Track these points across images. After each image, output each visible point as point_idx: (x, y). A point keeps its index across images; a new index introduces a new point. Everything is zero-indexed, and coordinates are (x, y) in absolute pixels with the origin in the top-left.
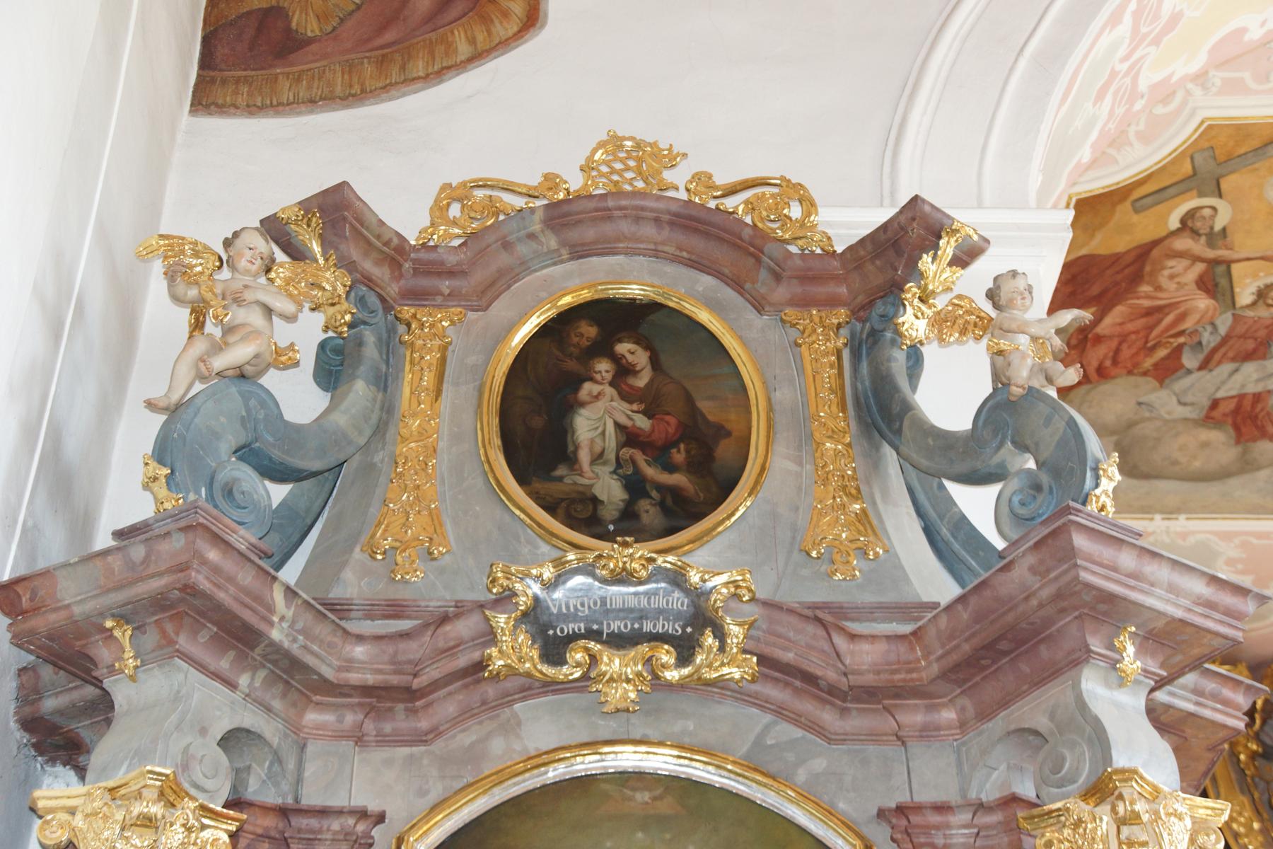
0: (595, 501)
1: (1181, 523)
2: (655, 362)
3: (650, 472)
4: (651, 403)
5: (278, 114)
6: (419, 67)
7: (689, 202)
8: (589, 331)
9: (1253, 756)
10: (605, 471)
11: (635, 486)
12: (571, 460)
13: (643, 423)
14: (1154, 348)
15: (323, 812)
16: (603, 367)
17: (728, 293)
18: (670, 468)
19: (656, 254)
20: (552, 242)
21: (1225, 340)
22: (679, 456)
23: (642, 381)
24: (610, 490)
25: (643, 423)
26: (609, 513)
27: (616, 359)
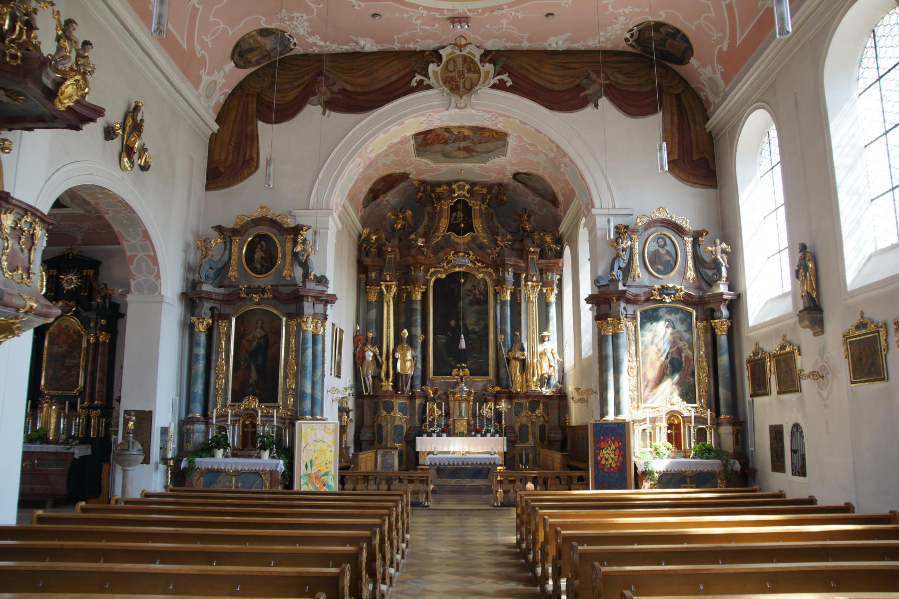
0: (256, 268)
1: (463, 165)
2: (266, 245)
3: (265, 264)
4: (265, 252)
5: (218, 190)
6: (239, 179)
7: (272, 218)
8: (257, 240)
9: (486, 209)
10: (258, 263)
11: (262, 266)
12: (254, 262)
13: (264, 255)
14: (441, 140)
15: (223, 314)
16: (259, 246)
17: (277, 232)
18: (267, 263)
19: (267, 226)
20: (253, 224)
21: (455, 139)
22: (268, 261)
23: (264, 248)
24: (259, 266)
25: (264, 255)
26: (259, 270)
27: (261, 244)
